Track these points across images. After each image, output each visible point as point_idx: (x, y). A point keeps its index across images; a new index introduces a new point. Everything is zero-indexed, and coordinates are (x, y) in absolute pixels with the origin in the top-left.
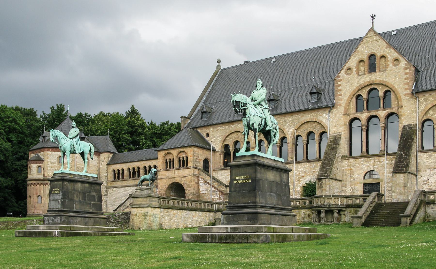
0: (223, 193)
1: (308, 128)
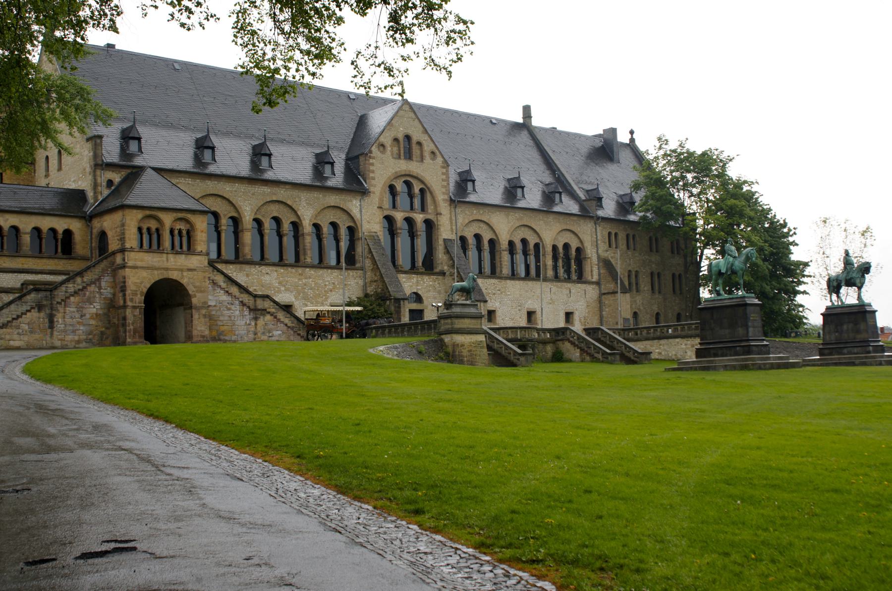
0: (249, 307)
1: (332, 216)
